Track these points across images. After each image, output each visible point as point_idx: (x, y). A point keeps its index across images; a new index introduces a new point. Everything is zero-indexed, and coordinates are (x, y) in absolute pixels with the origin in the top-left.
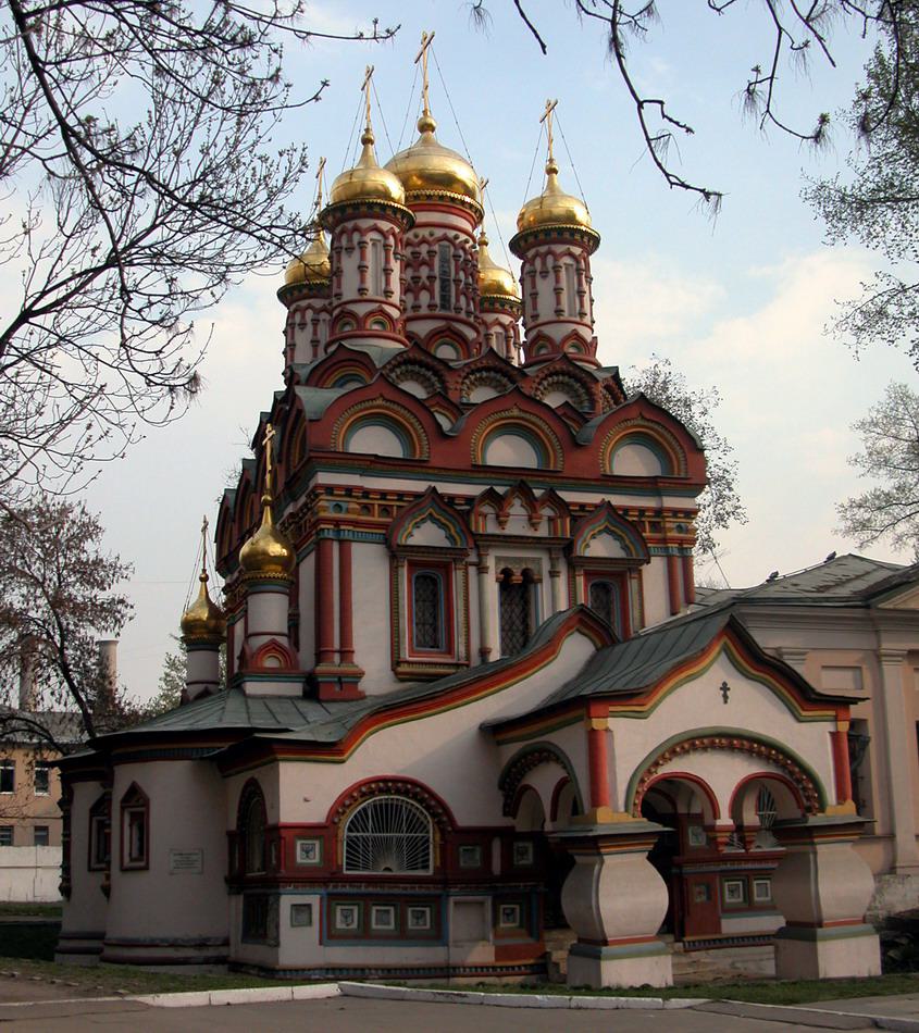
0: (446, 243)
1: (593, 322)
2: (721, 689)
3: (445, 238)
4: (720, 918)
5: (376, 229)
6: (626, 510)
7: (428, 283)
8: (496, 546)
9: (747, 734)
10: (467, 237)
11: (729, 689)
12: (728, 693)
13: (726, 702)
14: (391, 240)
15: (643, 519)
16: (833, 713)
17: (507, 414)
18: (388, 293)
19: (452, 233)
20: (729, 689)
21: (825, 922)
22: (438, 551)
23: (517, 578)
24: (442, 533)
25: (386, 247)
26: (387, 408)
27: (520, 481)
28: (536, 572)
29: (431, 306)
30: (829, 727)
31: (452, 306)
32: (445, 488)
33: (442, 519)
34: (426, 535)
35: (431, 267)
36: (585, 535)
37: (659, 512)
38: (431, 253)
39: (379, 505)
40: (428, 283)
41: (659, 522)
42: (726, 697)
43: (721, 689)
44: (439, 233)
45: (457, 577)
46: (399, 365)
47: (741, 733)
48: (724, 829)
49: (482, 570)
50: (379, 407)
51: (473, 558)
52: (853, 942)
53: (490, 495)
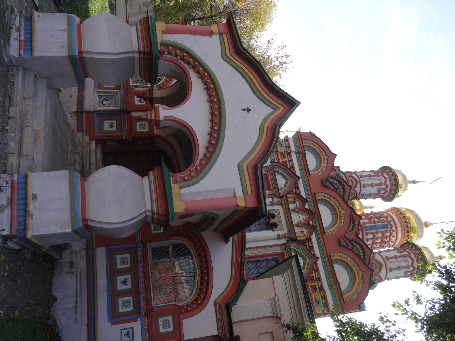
0: (390, 226)
1: (389, 279)
2: (248, 108)
3: (391, 226)
4: (106, 246)
5: (386, 179)
6: (317, 271)
9: (223, 121)
11: (248, 112)
12: (246, 111)
13: (242, 110)
14: (384, 187)
15: (316, 282)
16: (250, 192)
18: (365, 186)
19: (394, 228)
20: (248, 112)
21: (86, 183)
23: (273, 221)
24: (283, 187)
25: (380, 184)
26: (324, 160)
27: (314, 214)
28: (277, 229)
29: (364, 223)
30: (239, 194)
32: (300, 183)
33: (288, 184)
34: (281, 181)
35: (378, 222)
36: (300, 248)
37: (321, 288)
38: (383, 221)
42: (244, 110)
43: (248, 108)
44: (392, 223)
46: (340, 183)
47: (223, 118)
48: (157, 114)
49: (272, 205)
50: (324, 157)
51: (276, 200)
52: (66, 204)
53: (304, 201)
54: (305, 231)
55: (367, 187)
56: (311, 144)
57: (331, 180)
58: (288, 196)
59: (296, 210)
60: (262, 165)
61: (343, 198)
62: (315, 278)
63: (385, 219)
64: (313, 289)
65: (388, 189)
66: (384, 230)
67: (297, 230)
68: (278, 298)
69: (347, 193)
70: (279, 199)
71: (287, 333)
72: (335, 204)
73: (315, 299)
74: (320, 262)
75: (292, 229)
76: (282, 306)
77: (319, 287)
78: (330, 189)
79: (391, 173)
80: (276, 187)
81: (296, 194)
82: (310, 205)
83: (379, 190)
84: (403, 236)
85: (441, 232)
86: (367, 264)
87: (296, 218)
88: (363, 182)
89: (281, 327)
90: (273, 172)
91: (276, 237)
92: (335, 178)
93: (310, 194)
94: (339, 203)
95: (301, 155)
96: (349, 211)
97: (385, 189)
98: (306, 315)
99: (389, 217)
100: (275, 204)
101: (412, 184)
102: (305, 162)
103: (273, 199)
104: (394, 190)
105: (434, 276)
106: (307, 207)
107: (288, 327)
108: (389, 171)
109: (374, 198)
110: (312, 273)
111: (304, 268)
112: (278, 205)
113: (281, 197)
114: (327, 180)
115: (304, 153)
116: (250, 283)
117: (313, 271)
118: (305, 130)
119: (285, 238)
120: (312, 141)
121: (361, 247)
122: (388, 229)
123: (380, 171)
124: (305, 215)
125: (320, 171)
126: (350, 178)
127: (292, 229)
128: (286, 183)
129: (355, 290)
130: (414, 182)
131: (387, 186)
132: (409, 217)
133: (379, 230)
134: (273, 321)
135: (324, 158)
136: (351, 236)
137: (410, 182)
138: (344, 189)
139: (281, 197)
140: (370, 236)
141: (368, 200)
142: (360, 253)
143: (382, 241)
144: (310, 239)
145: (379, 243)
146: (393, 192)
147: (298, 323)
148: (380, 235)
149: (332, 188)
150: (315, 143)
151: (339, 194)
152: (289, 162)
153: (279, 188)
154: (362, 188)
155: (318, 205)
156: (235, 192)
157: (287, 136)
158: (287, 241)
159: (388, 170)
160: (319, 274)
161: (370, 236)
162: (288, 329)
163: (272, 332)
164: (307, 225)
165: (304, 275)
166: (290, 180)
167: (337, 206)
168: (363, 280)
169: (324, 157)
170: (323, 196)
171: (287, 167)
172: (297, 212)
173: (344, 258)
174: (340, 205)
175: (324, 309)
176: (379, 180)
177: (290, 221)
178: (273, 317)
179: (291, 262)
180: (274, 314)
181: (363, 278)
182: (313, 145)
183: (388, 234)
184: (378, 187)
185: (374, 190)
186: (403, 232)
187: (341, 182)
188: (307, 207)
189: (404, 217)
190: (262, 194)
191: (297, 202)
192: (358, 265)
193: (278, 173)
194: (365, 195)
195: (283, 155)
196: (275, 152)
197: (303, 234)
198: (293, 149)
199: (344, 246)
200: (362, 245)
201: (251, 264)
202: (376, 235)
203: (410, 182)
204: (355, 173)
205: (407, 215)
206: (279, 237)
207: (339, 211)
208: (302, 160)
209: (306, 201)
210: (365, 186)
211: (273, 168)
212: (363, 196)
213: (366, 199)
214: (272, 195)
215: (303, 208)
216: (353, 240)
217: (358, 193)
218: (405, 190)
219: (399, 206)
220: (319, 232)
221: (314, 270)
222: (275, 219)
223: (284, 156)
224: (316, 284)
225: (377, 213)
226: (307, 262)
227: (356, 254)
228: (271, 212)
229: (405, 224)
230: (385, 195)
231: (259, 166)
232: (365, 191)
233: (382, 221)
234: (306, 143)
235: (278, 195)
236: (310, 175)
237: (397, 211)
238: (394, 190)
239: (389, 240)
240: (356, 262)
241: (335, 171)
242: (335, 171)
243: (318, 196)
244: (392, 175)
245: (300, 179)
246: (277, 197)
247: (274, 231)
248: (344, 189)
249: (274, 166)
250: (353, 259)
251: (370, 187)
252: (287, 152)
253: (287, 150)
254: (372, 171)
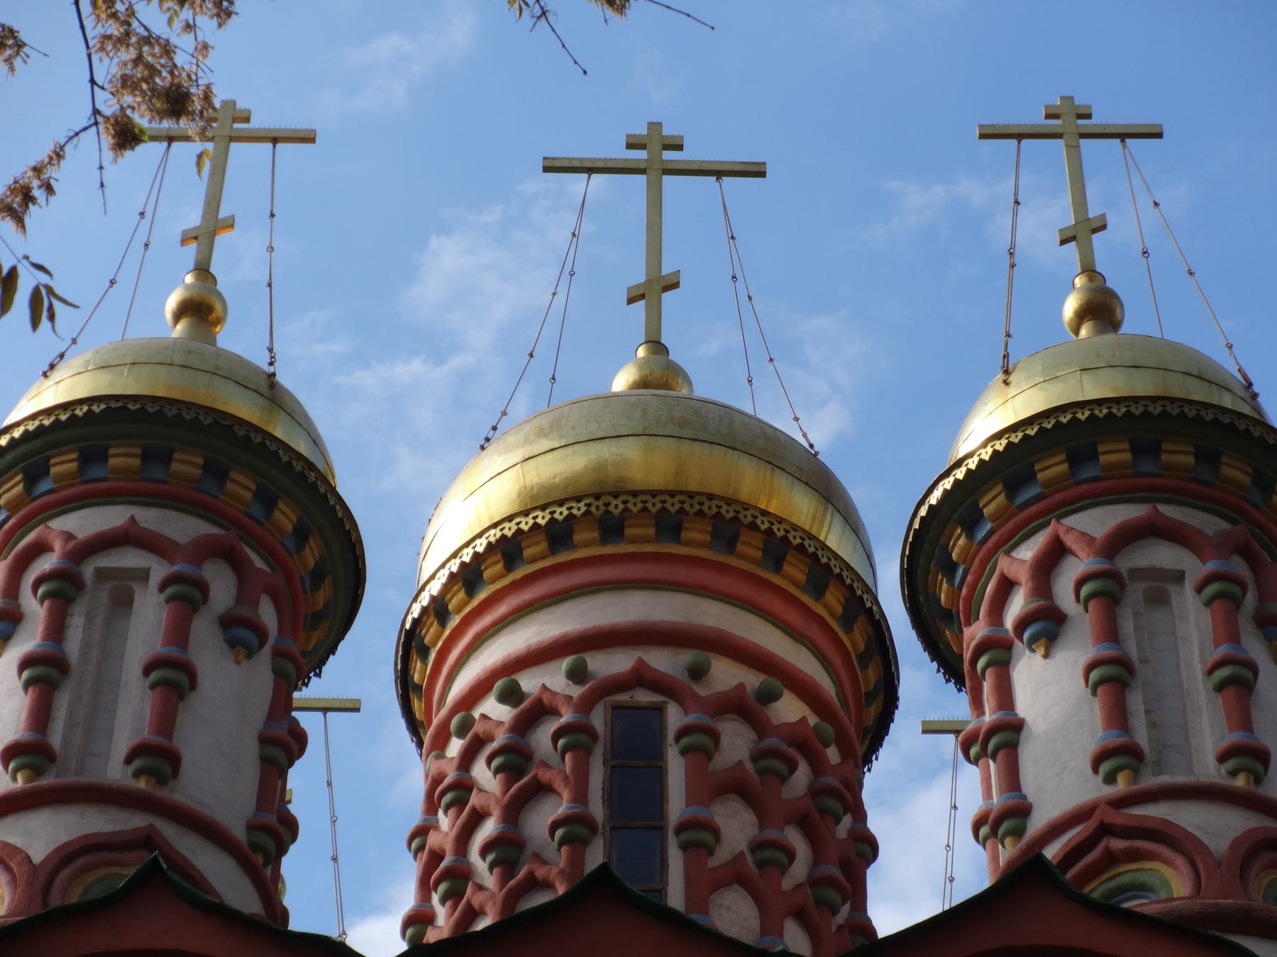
0: (644, 697)
3: (640, 678)
83: (239, 632)
122: (675, 717)
133: (676, 806)
184: (204, 630)
185: (229, 688)
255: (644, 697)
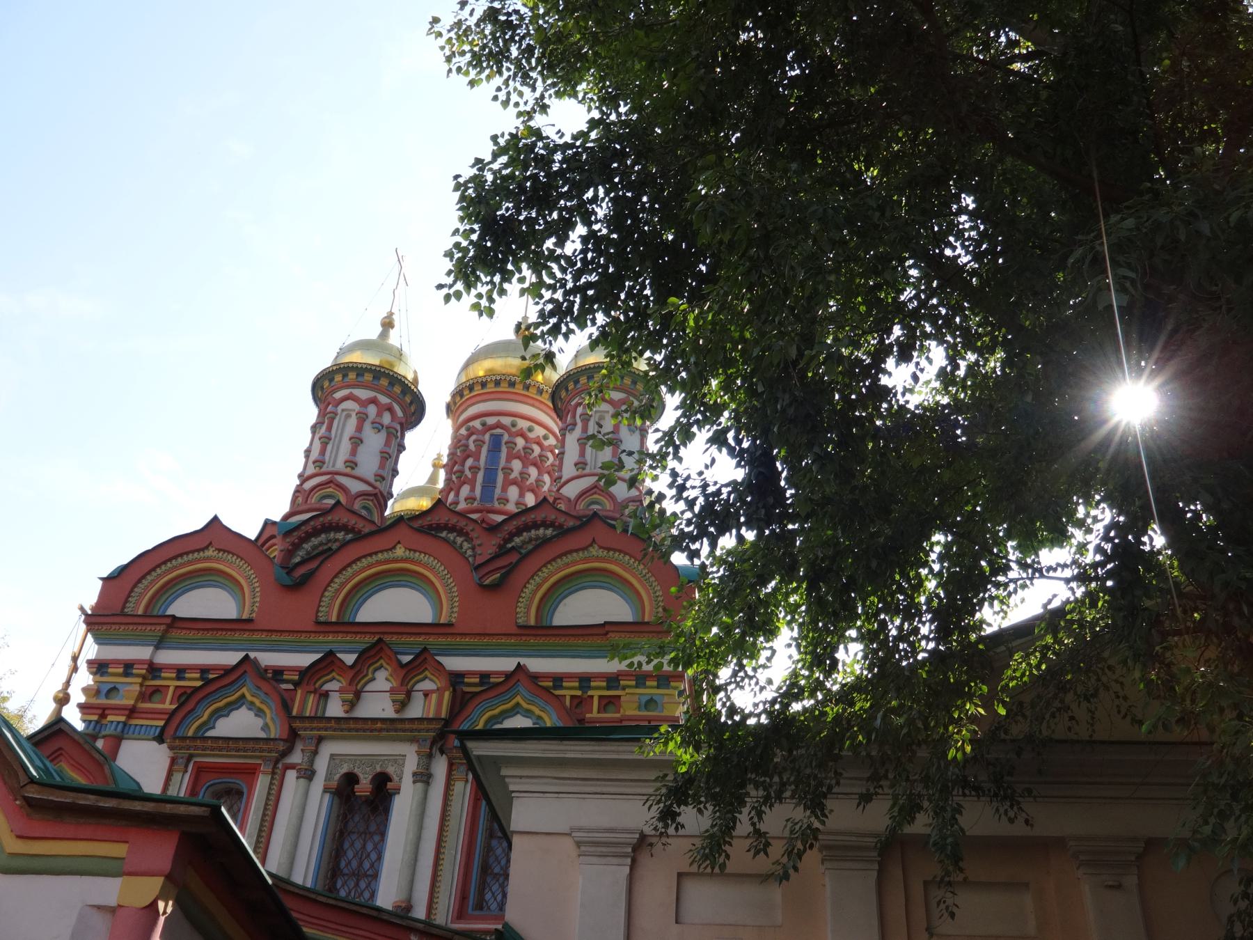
0: (499, 431)
3: (498, 425)
6: (558, 679)
7: (470, 476)
8: (333, 738)
10: (528, 424)
14: (372, 410)
15: (590, 693)
16: (119, 850)
17: (390, 555)
18: (351, 464)
19: (506, 421)
22: (241, 745)
23: (365, 786)
24: (259, 722)
25: (362, 418)
26: (218, 560)
27: (381, 642)
28: (396, 778)
29: (470, 499)
30: (109, 890)
31: (496, 496)
32: (268, 659)
33: (257, 702)
34: (241, 723)
35: (477, 459)
37: (613, 680)
38: (479, 444)
39: (177, 687)
40: (470, 476)
41: (619, 697)
44: (491, 421)
45: (262, 783)
46: (316, 532)
50: (208, 559)
51: (296, 757)
53: (328, 663)
54: (427, 685)
55: (359, 458)
56: (147, 588)
57: (297, 560)
58: (294, 713)
59: (350, 696)
60: (32, 780)
61: (360, 537)
62: (579, 693)
63: (474, 437)
64: (611, 708)
65: (384, 400)
66: (504, 450)
67: (416, 710)
68: (580, 829)
69: (353, 521)
70: (299, 746)
71: (683, 826)
72: (370, 566)
73: (639, 708)
74: (536, 665)
75: (407, 726)
76: (605, 822)
77: (608, 688)
78: (316, 569)
79: (338, 378)
80: (251, 745)
81: (297, 684)
82: (348, 646)
83: (378, 426)
84: (537, 404)
85: (445, 291)
86: (578, 523)
87: (378, 702)
88: (340, 466)
89: (664, 840)
90: (198, 743)
91: (419, 785)
92: (293, 544)
93: (313, 638)
94: (370, 555)
95: (174, 634)
96: (403, 531)
97: (382, 409)
98: (621, 749)
99: (471, 424)
100: (312, 762)
101: (392, 332)
102: (208, 626)
103: (292, 767)
104: (392, 384)
105: (561, 350)
106: (349, 659)
107: (668, 816)
108: (331, 380)
109: (401, 448)
110: (560, 698)
111: (539, 717)
112: (315, 753)
113: (293, 737)
114: (290, 571)
115: (168, 621)
116: (513, 915)
117: (557, 692)
118: (90, 596)
119: (430, 756)
120: (139, 581)
121: (527, 528)
122: (506, 437)
123: (322, 406)
124: (376, 670)
125: (251, 584)
126: (313, 500)
127: (407, 726)
128: (251, 706)
129: (640, 581)
130: (388, 324)
131: (373, 401)
132: (486, 371)
133: (503, 463)
134: (644, 859)
135: (212, 559)
136: (489, 546)
137: (384, 334)
138: (337, 528)
139: (293, 737)
140: (513, 492)
141: (400, 467)
142: (537, 538)
143: (535, 465)
144: (456, 678)
145: (540, 474)
146: (397, 389)
147: (656, 780)
148: (517, 465)
149: (313, 565)
150: (149, 573)
151: (345, 544)
152: (183, 679)
153: (263, 735)
154: (357, 472)
155: (358, 620)
156: (99, 907)
157: (90, 663)
158: (442, 752)
159: (326, 384)
160: (570, 676)
161: (513, 492)
162: (673, 820)
163: (680, 875)
164: (408, 674)
165: (560, 724)
166: (244, 690)
167: (379, 563)
168: (615, 550)
169: (208, 559)
170: (334, 598)
171: (197, 689)
172: (358, 695)
173: (539, 586)
174: (376, 553)
175: (675, 688)
176: (348, 416)
177: (379, 725)
178: (634, 861)
179: (479, 757)
180: (625, 856)
181: (609, 549)
182: (153, 582)
183: (520, 442)
184: (367, 426)
186: (521, 398)
187: (314, 528)
188: (349, 659)
189: (484, 385)
190: (137, 806)
191: (327, 687)
192: (570, 552)
193: (209, 724)
194: (381, 472)
195: (149, 694)
196: (129, 717)
197: (434, 697)
198: (141, 653)
199: (505, 577)
200: (524, 520)
201: (488, 896)
202: (512, 476)
203: (384, 334)
204: (303, 478)
205: (481, 373)
206: (424, 777)
207: (396, 561)
208: (191, 635)
209: (330, 655)
210: (351, 464)
211: (184, 738)
212: (384, 479)
213: (395, 472)
214: (275, 767)
215: (352, 673)
216: (500, 547)
217: (370, 489)
218: (400, 355)
219: (451, 386)
220: (442, 640)
221: (555, 687)
222: (361, 776)
223: (157, 690)
224: (596, 694)
225: (452, 455)
226: (525, 705)
227: (536, 548)
228: (334, 784)
229: (504, 387)
230: (400, 414)
231: (33, 793)
232: (368, 464)
233: (479, 448)
234: (138, 603)
235: (281, 746)
236: (250, 621)
237: (462, 396)
238: (392, 384)
239: (539, 444)
240: (560, 556)
241: (273, 537)
242: (273, 537)
243: (328, 613)
244: (345, 376)
245: (252, 655)
246: (288, 751)
247: (397, 790)
248: (337, 528)
249: (180, 733)
250: (549, 562)
251: (361, 449)
252: (144, 678)
253: (138, 676)
254: (314, 429)
255: (499, 431)
